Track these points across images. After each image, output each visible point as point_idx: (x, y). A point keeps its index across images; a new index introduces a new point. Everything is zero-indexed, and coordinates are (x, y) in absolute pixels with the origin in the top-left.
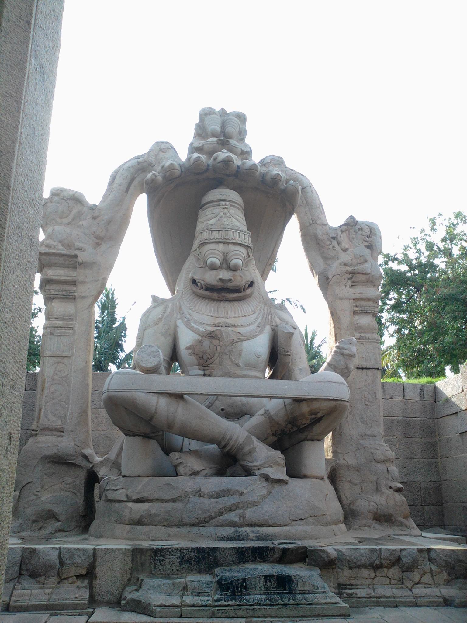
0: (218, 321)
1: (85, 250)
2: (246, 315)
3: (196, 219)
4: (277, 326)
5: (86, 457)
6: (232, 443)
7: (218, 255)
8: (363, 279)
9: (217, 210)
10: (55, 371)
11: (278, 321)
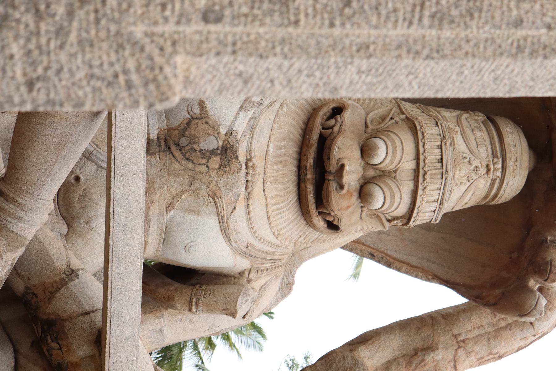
0: (258, 162)
2: (271, 219)
4: (249, 281)
6: (10, 207)
7: (392, 161)
9: (484, 152)
11: (257, 284)
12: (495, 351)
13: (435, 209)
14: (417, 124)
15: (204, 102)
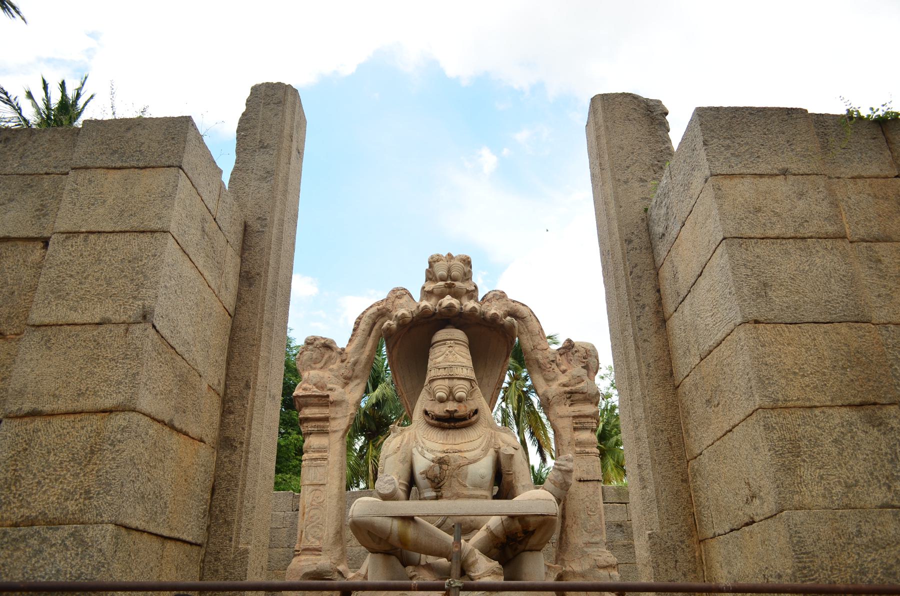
1: (335, 390)
4: (500, 448)
5: (340, 573)
7: (445, 389)
8: (581, 397)
9: (444, 349)
11: (501, 444)
12: (538, 333)
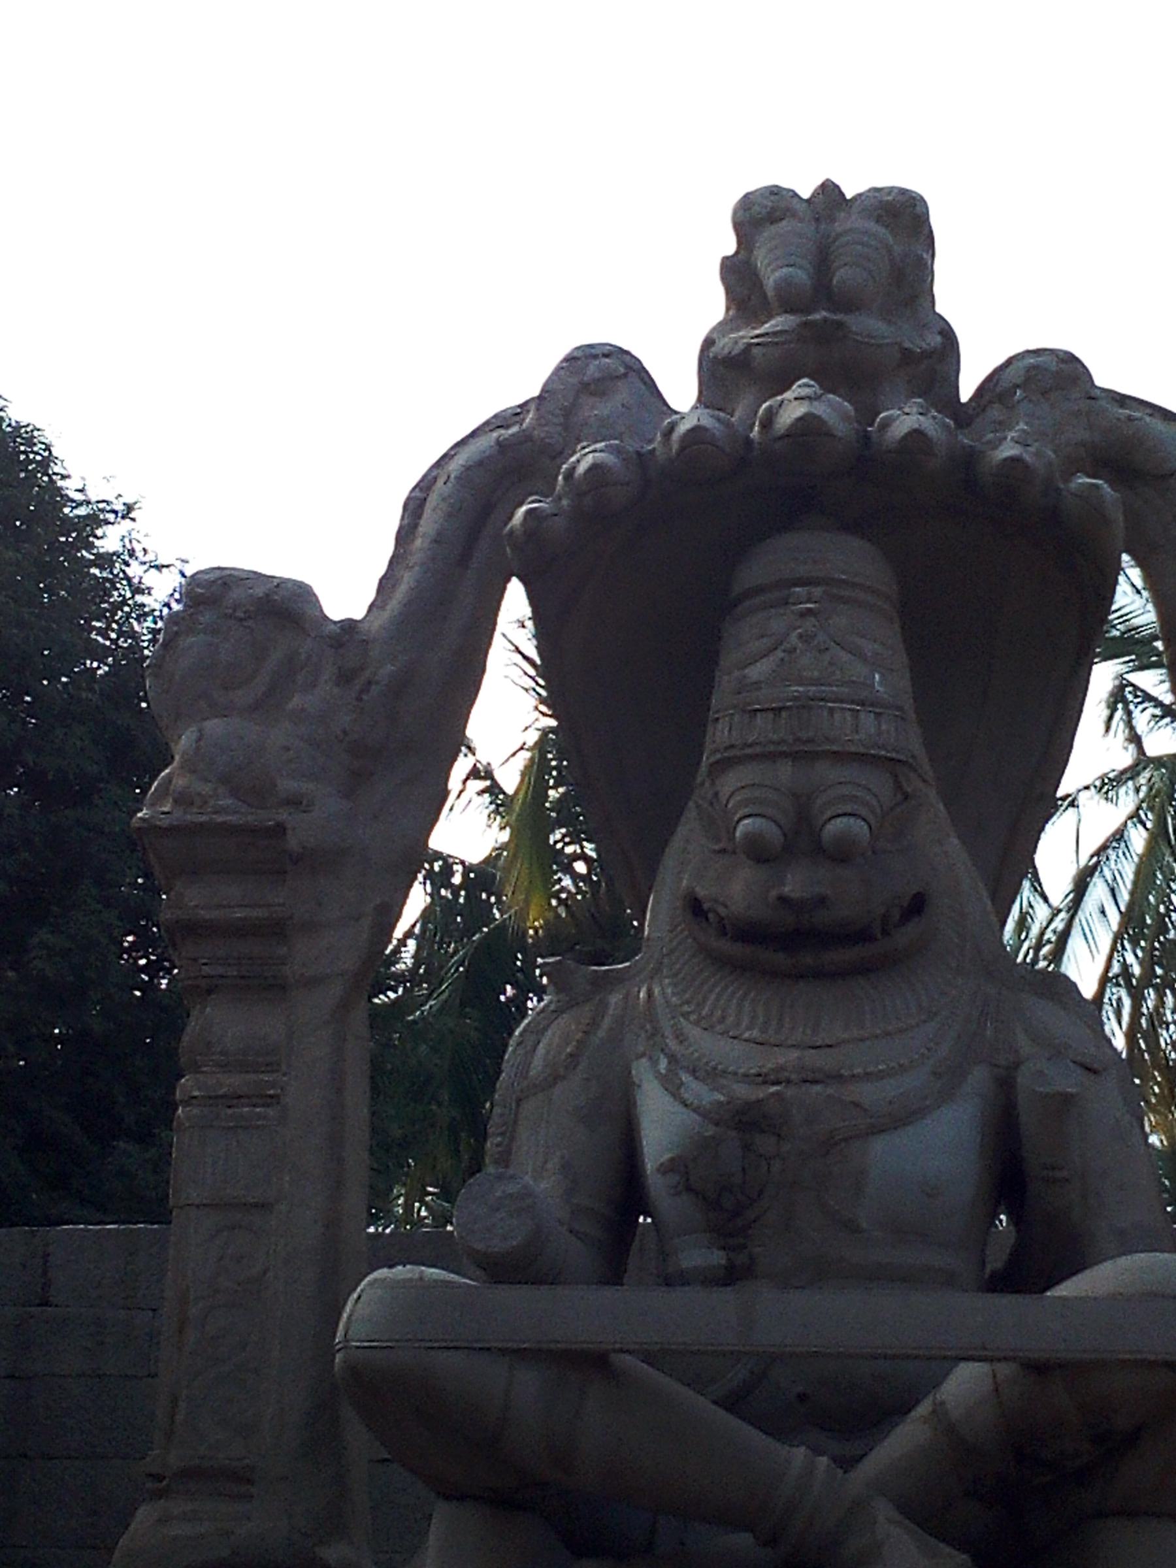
3: (710, 660)
4: (1017, 1065)
10: (221, 1258)
13: (872, 715)
14: (712, 760)
15: (662, 1165)
